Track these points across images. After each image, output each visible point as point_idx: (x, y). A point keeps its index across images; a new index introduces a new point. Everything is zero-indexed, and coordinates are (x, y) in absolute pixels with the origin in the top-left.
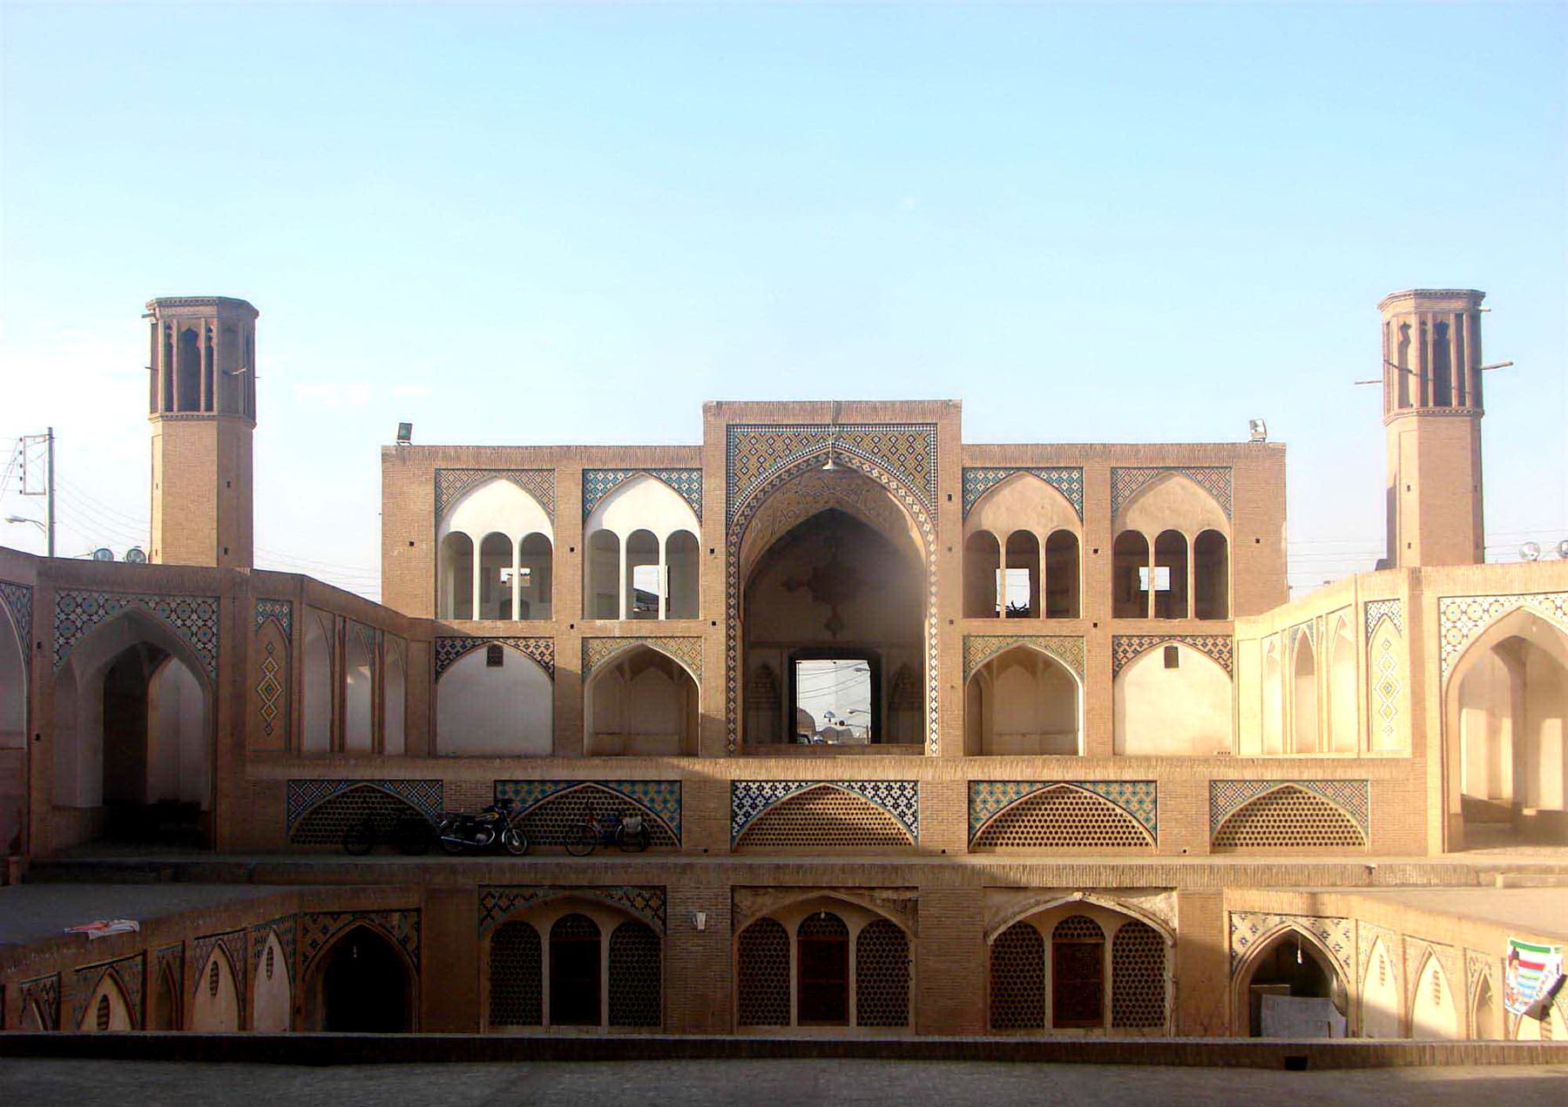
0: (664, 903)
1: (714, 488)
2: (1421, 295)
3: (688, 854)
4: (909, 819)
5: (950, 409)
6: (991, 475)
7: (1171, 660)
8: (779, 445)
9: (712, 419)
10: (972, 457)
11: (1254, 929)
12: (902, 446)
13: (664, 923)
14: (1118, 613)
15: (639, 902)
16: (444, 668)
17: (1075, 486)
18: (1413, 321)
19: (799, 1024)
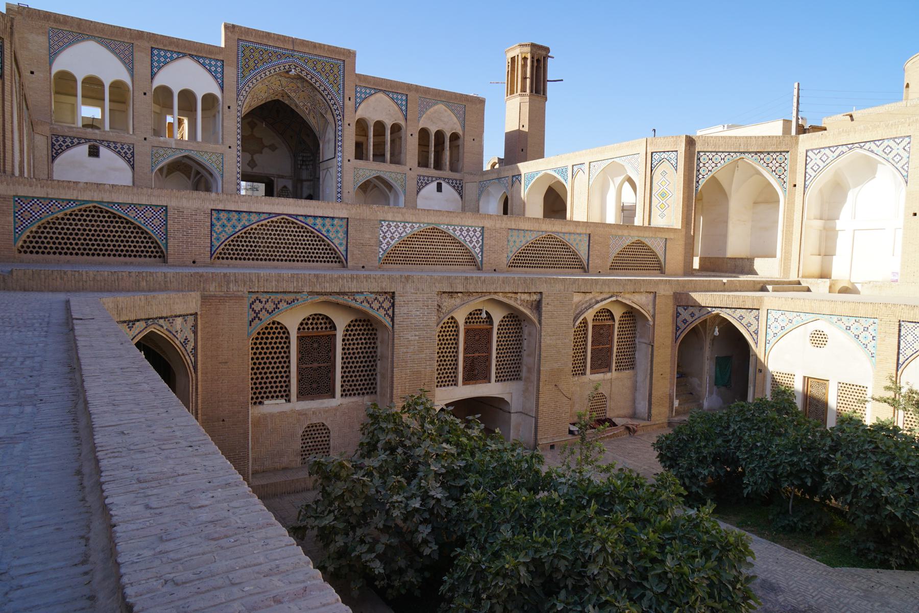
0: (393, 305)
1: (231, 73)
2: (533, 46)
3: (355, 268)
4: (478, 250)
5: (350, 55)
6: (368, 91)
7: (439, 188)
8: (265, 56)
9: (229, 34)
10: (360, 80)
11: (692, 315)
12: (327, 68)
13: (393, 320)
14: (420, 165)
15: (376, 305)
16: (58, 154)
17: (404, 103)
18: (529, 56)
19: (464, 384)
